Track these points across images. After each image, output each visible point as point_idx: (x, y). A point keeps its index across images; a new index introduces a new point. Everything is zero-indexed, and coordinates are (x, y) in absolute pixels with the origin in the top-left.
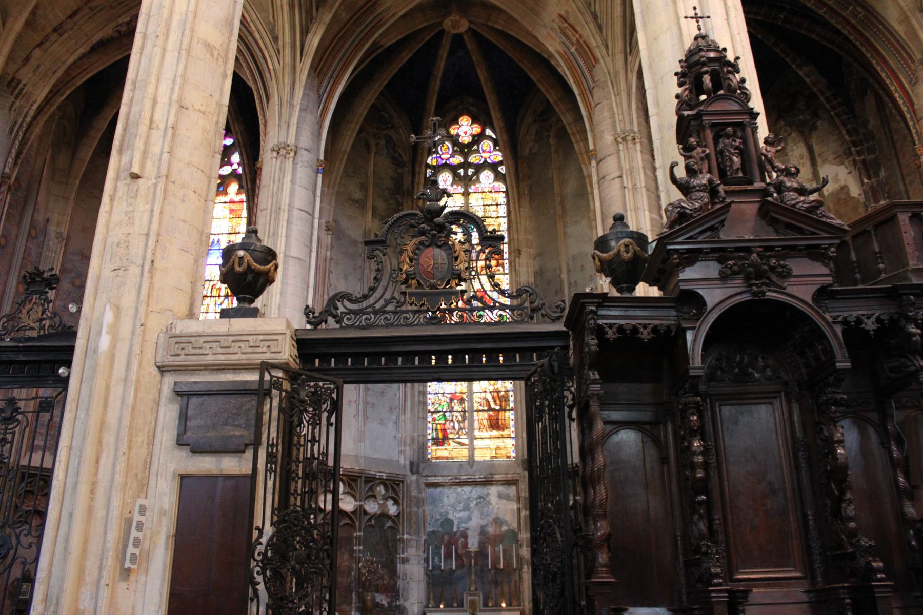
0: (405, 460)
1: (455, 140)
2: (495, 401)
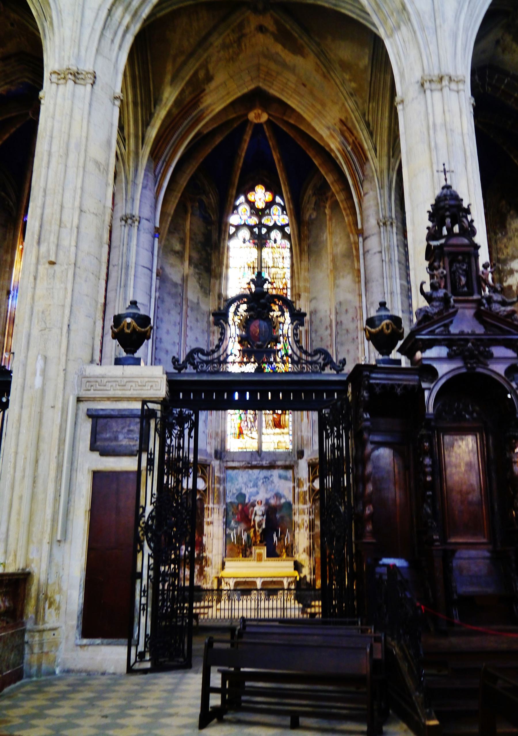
0: (211, 449)
1: (252, 205)
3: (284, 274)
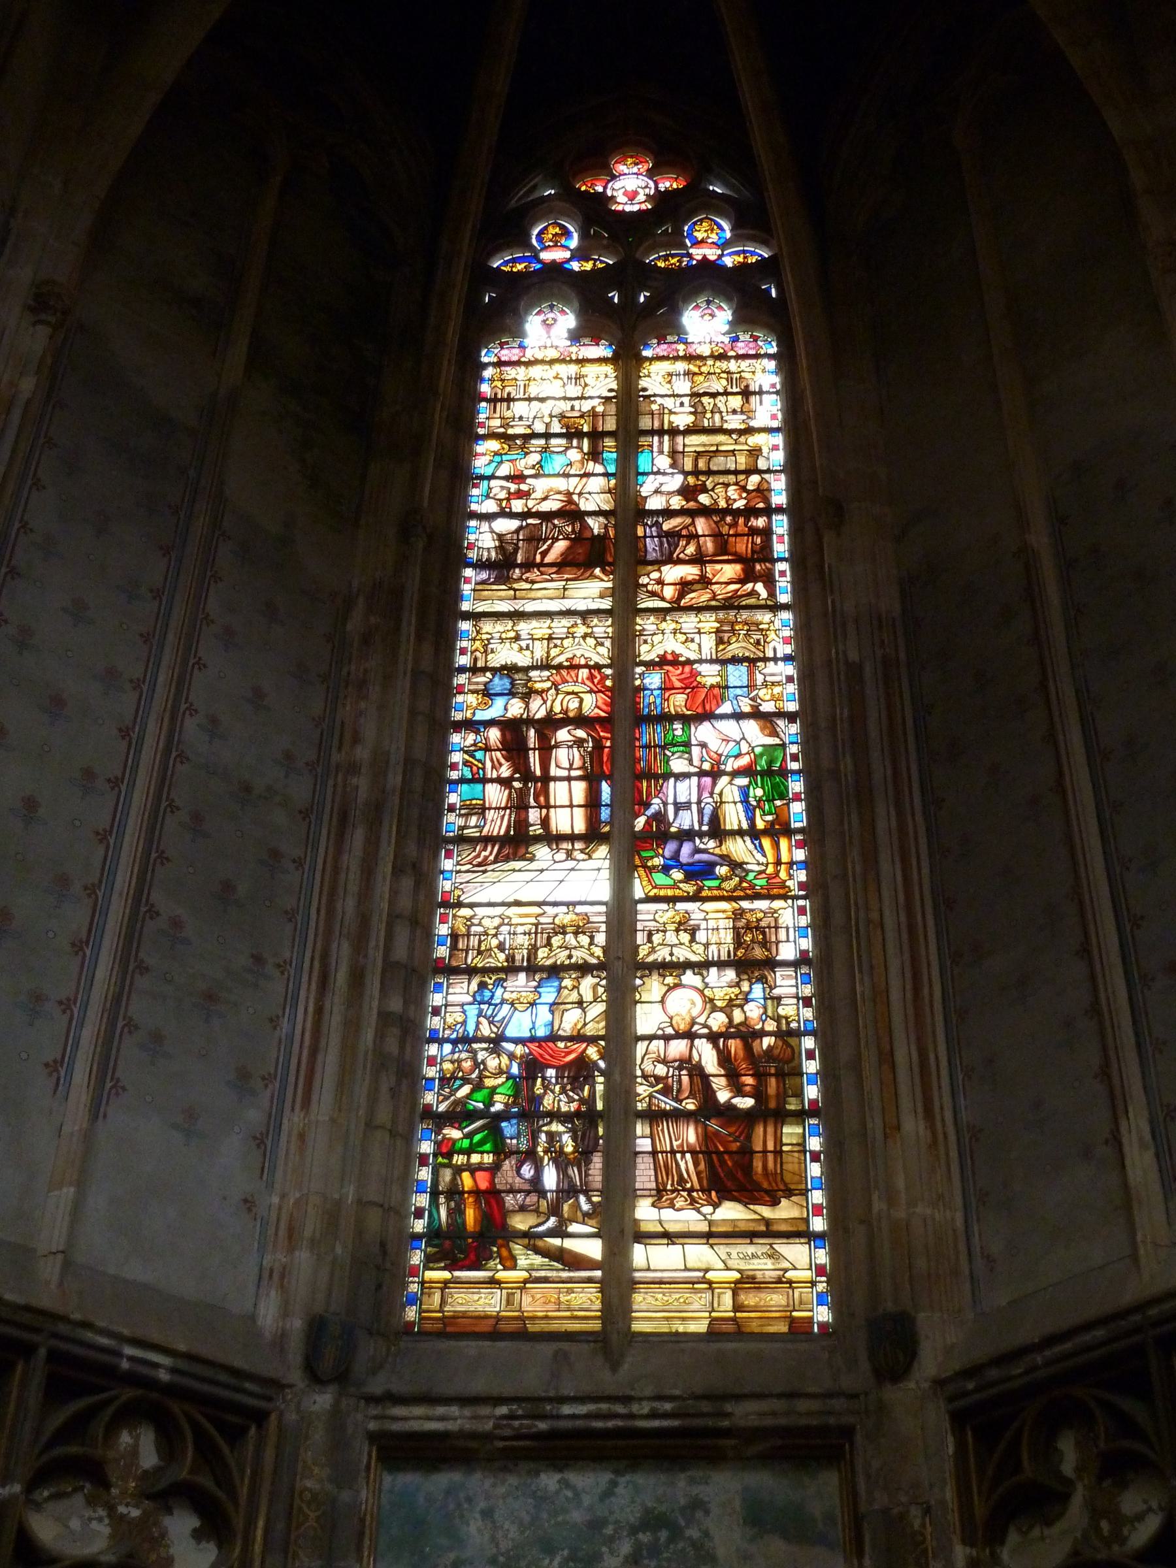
0: (285, 1312)
2: (733, 1077)
3: (755, 453)
